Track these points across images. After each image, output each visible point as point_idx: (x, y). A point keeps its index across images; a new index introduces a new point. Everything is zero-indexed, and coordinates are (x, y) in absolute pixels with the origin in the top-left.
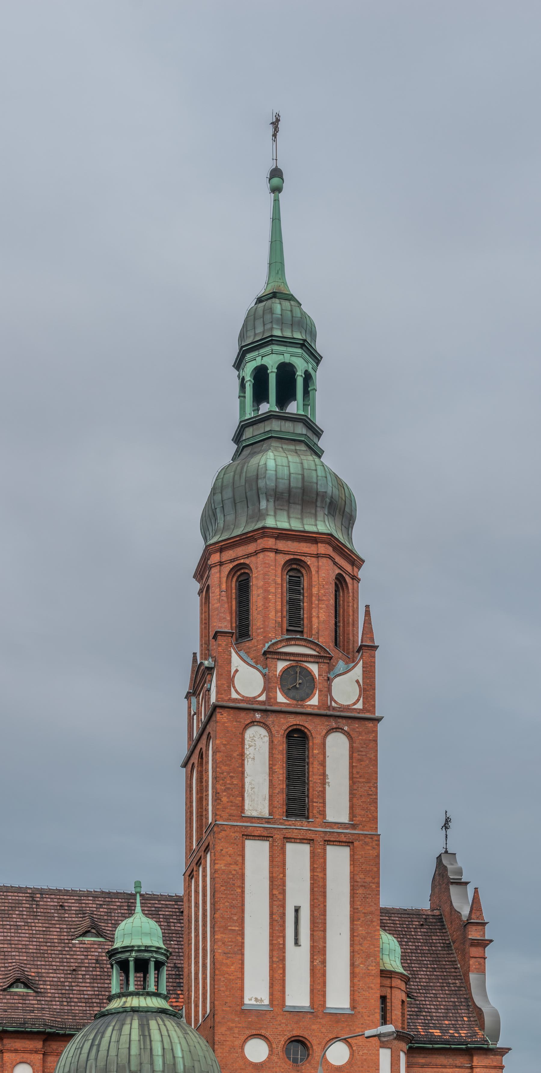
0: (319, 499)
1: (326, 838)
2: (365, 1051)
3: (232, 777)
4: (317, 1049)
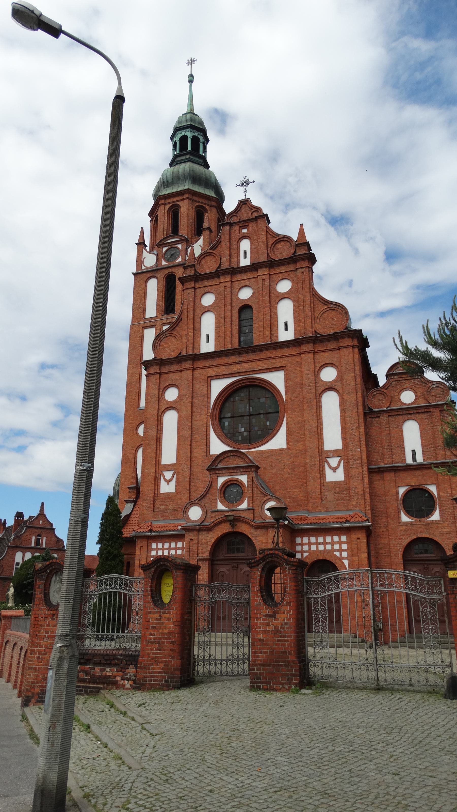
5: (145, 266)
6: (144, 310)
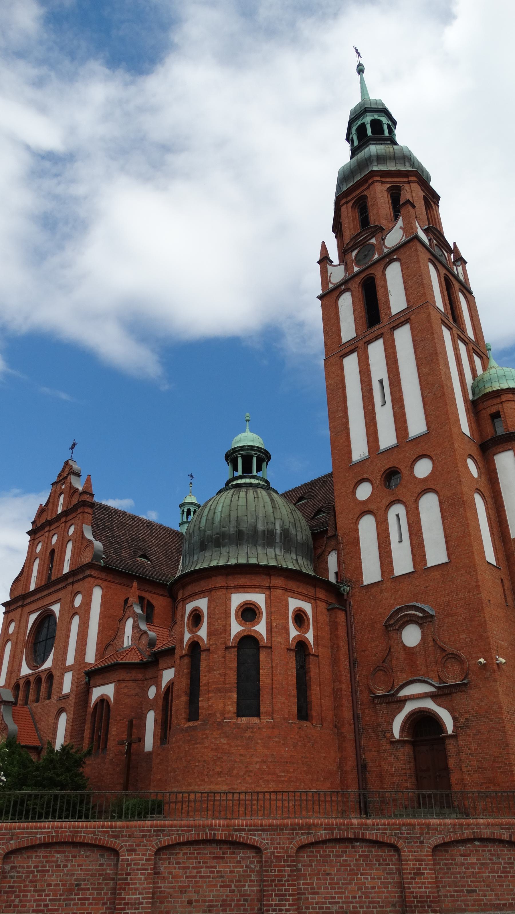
0: (368, 162)
1: (391, 327)
2: (443, 457)
3: (331, 329)
4: (405, 471)
5: (332, 284)
6: (340, 336)
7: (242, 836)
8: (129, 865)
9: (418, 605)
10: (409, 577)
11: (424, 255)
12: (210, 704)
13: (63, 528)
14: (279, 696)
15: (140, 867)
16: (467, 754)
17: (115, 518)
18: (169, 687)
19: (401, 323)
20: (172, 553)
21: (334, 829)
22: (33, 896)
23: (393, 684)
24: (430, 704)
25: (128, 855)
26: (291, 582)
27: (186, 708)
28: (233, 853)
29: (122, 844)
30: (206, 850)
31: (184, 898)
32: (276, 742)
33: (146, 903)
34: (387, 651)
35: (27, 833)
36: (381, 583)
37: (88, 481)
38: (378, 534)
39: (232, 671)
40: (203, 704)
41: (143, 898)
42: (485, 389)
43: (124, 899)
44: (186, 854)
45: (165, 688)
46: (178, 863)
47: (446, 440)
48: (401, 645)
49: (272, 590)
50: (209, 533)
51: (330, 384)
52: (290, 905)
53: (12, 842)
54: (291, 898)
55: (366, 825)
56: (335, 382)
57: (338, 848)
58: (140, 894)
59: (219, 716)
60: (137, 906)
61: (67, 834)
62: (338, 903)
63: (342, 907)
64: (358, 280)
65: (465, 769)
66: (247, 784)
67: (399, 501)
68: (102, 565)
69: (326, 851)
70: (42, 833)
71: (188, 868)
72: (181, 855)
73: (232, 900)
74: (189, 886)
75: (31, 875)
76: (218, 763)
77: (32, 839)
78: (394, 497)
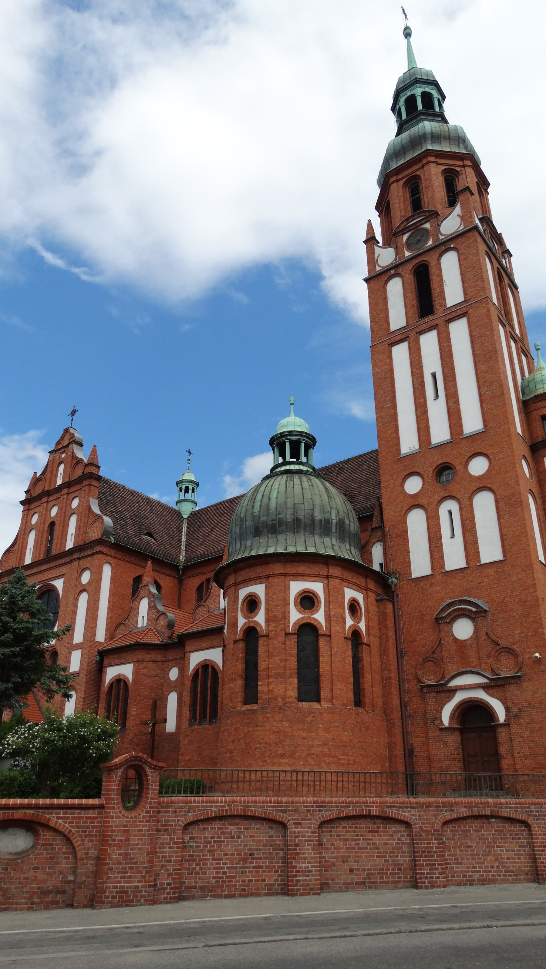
0: (422, 139)
1: (447, 319)
2: (501, 456)
4: (459, 468)
5: (380, 266)
7: (394, 812)
8: (297, 837)
9: (471, 599)
10: (462, 573)
11: (482, 248)
12: (270, 688)
13: (65, 500)
14: (338, 683)
15: (307, 838)
16: (519, 742)
17: (116, 492)
18: (198, 669)
19: (457, 316)
20: (173, 531)
21: (473, 807)
22: (212, 864)
23: (443, 674)
24: (481, 695)
25: (295, 828)
26: (346, 572)
27: (242, 692)
28: (386, 827)
29: (289, 818)
30: (362, 824)
31: (346, 867)
32: (336, 727)
33: (315, 871)
34: (437, 643)
35: (203, 806)
36: (430, 577)
37: (94, 452)
38: (428, 529)
39: (293, 658)
40: (262, 688)
41: (312, 867)
42: (536, 389)
43: (295, 867)
44: (345, 827)
45: (193, 669)
46: (339, 836)
47: (505, 439)
48: (452, 638)
49: (330, 579)
50: (264, 519)
51: (378, 373)
52: (439, 873)
53: (190, 814)
54: (440, 867)
55: (500, 803)
56: (382, 371)
57: (476, 824)
58: (309, 863)
59: (280, 700)
60: (307, 873)
61: (239, 808)
62: (479, 872)
63: (482, 876)
64: (410, 266)
65: (516, 755)
66: (310, 765)
67: (452, 497)
68: (113, 542)
69: (466, 827)
70: (216, 807)
71: (348, 840)
72: (341, 828)
73: (388, 869)
74: (349, 857)
75: (209, 845)
76: (280, 746)
77: (208, 812)
78: (447, 493)
